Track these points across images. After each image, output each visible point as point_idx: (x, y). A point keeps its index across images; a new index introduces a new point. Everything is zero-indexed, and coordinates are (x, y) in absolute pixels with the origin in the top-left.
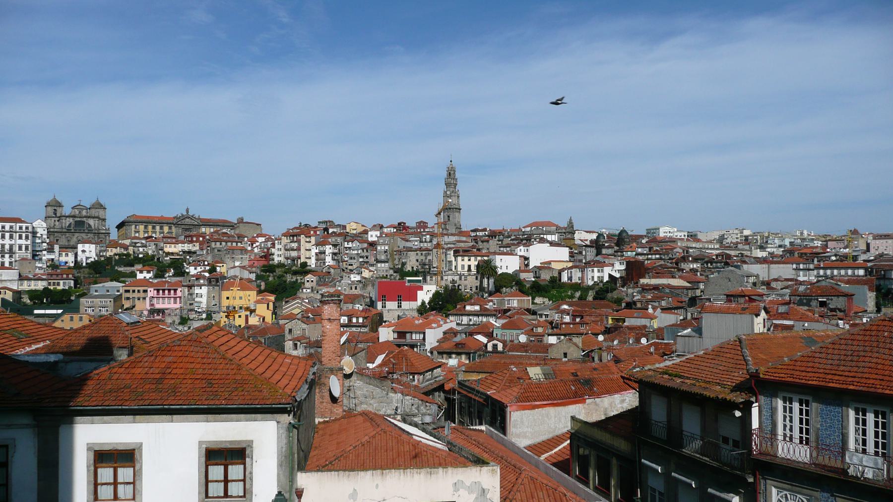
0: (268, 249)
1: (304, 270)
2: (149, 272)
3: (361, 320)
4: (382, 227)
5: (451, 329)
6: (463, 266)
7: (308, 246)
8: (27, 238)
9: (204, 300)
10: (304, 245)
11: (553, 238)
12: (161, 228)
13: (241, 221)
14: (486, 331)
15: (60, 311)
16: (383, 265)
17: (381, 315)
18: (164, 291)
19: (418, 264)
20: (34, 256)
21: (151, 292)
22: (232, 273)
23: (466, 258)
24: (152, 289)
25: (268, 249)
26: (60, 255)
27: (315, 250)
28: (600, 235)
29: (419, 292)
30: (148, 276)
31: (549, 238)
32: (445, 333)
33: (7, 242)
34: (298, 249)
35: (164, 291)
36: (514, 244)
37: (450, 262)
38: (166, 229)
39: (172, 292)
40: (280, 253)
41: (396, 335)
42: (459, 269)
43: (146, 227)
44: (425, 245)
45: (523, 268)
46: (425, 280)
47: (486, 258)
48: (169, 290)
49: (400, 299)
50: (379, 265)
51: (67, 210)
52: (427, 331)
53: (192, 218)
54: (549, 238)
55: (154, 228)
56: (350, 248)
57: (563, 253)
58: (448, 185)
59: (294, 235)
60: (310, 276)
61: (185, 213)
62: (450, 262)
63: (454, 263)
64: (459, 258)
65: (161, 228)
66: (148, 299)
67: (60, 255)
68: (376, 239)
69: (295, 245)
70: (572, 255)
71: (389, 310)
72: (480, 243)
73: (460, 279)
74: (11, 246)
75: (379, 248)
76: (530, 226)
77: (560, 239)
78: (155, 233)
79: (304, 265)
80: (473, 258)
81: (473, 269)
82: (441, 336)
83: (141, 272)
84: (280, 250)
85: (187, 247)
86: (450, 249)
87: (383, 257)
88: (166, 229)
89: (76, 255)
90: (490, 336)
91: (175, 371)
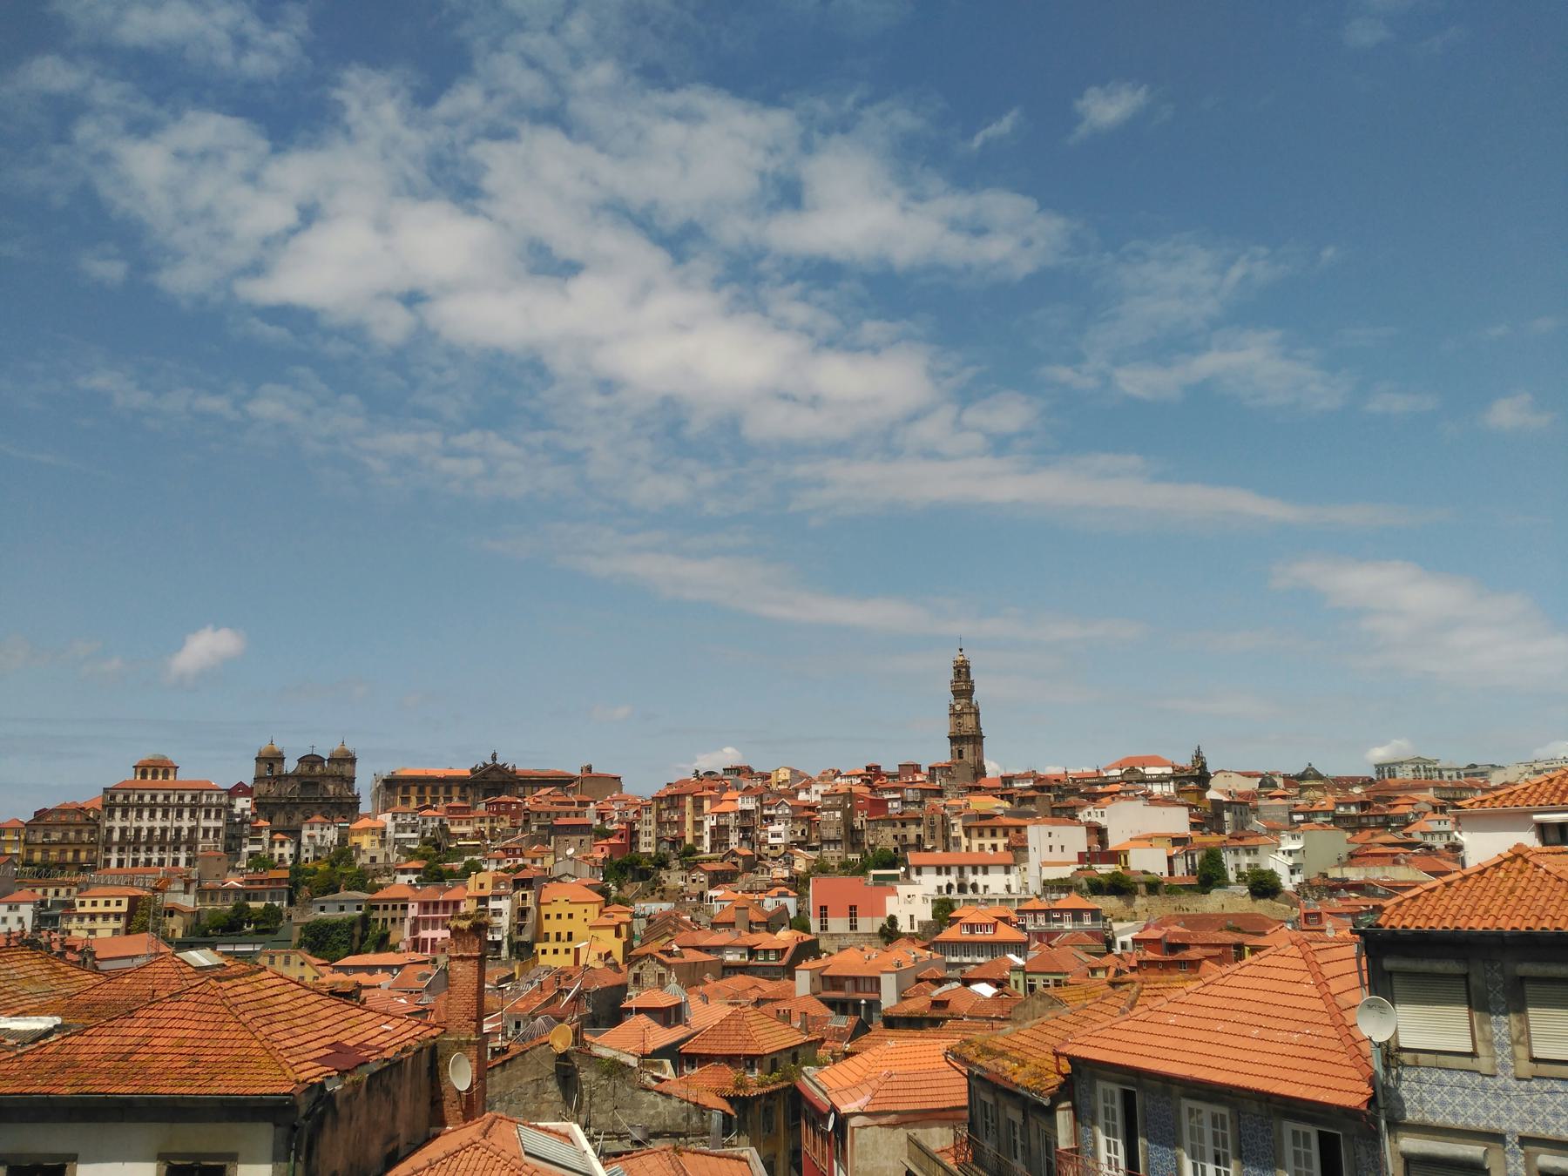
0: (631, 824)
1: (690, 859)
2: (415, 871)
3: (772, 957)
4: (838, 774)
6: (981, 847)
8: (218, 816)
9: (504, 921)
12: (448, 791)
14: (996, 976)
15: (258, 948)
17: (815, 942)
19: (896, 844)
20: (228, 849)
21: (413, 911)
25: (631, 824)
26: (272, 844)
27: (709, 823)
28: (1267, 781)
30: (413, 878)
33: (186, 823)
34: (680, 824)
37: (957, 839)
38: (456, 791)
42: (975, 849)
43: (421, 790)
45: (1097, 847)
46: (907, 874)
51: (290, 766)
52: (883, 978)
54: (1157, 789)
56: (772, 818)
57: (1177, 821)
58: (957, 694)
59: (673, 800)
61: (489, 762)
62: (957, 839)
63: (964, 841)
66: (407, 924)
67: (272, 844)
72: (1016, 801)
74: (192, 830)
77: (1178, 792)
79: (691, 851)
81: (1001, 848)
83: (404, 872)
84: (648, 823)
87: (831, 833)
88: (456, 791)
89: (299, 844)
90: (999, 984)
91: (155, 1042)
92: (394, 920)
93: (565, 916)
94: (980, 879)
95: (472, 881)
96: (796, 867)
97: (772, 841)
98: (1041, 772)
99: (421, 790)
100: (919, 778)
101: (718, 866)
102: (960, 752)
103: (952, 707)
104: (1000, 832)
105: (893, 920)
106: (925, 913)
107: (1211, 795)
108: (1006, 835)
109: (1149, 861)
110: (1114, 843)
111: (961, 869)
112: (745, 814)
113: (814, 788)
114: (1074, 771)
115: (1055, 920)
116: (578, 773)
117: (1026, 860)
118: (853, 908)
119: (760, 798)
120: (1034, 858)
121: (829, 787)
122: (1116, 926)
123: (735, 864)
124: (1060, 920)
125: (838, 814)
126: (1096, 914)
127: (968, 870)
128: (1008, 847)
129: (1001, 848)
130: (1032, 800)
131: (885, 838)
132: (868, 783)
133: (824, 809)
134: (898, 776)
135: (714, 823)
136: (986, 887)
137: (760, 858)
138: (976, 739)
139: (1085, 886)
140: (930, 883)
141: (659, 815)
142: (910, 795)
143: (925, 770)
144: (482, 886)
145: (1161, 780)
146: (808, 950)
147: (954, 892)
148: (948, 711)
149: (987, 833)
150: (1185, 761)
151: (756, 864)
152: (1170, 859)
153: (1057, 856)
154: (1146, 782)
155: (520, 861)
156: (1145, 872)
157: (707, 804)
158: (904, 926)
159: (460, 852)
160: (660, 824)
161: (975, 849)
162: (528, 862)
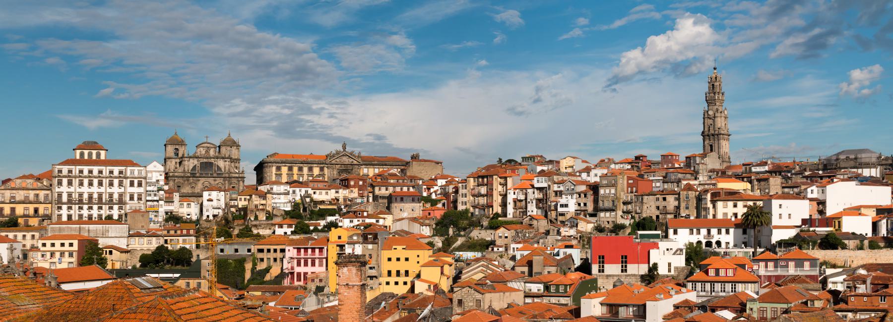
2: (290, 226)
4: (611, 161)
6: (725, 214)
10: (498, 189)
11: (874, 172)
12: (310, 169)
13: (415, 158)
16: (608, 214)
17: (595, 280)
18: (306, 249)
19: (658, 213)
21: (291, 252)
22: (398, 226)
23: (731, 204)
24: (291, 248)
29: (651, 251)
30: (289, 231)
31: (866, 172)
32: (676, 307)
34: (489, 194)
35: (306, 249)
36: (804, 184)
38: (316, 171)
39: (317, 251)
40: (465, 199)
41: (605, 309)
42: (720, 216)
43: (290, 169)
45: (816, 216)
46: (666, 236)
47: (760, 203)
48: (313, 249)
49: (624, 261)
50: (602, 214)
52: (648, 304)
53: (351, 155)
54: (866, 172)
55: (300, 169)
56: (561, 192)
60: (502, 229)
63: (711, 211)
64: (720, 204)
65: (310, 169)
68: (598, 179)
69: (483, 190)
71: (608, 276)
75: (602, 191)
78: (302, 175)
80: (740, 204)
82: (671, 309)
83: (281, 226)
85: (343, 193)
86: (706, 191)
87: (608, 204)
88: (316, 171)
92: (275, 260)
93: (402, 259)
95: (333, 234)
96: (579, 228)
97: (560, 210)
99: (290, 169)
100: (677, 166)
102: (711, 146)
105: (655, 266)
106: (680, 261)
110: (830, 211)
111: (709, 232)
112: (540, 189)
113: (593, 172)
115: (782, 267)
116: (409, 159)
121: (605, 171)
122: (829, 271)
123: (531, 225)
125: (613, 191)
126: (813, 262)
127: (714, 231)
129: (739, 217)
131: (650, 209)
135: (515, 197)
140: (683, 238)
144: (340, 237)
146: (588, 287)
154: (857, 168)
155: (368, 221)
156: (853, 234)
158: (662, 270)
159: (322, 214)
162: (373, 221)
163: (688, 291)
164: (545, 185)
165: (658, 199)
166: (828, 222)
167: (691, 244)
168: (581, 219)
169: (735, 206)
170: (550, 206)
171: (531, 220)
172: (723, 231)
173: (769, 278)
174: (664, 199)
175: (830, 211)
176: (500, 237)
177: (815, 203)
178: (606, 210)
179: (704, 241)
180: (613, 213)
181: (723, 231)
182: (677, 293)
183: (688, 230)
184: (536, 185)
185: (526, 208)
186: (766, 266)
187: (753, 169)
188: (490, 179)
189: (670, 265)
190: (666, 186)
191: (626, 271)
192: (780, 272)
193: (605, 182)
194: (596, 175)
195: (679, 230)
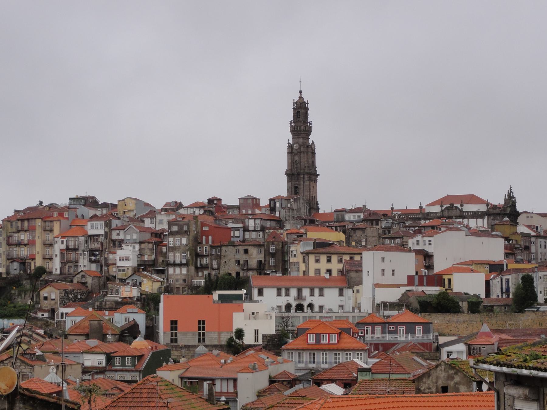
3: (129, 362)
4: (179, 206)
5: (284, 373)
6: (318, 271)
7: (50, 237)
14: (345, 377)
16: (178, 270)
19: (238, 269)
27: (59, 246)
29: (234, 313)
32: (272, 381)
34: (31, 243)
42: (312, 273)
44: (254, 235)
45: (424, 271)
50: (171, 271)
52: (241, 377)
54: (472, 223)
57: (494, 250)
60: (48, 289)
63: (302, 267)
64: (312, 259)
69: (24, 237)
70: (510, 252)
73: (312, 294)
76: (440, 202)
81: (335, 273)
82: (265, 384)
94: (317, 301)
97: (119, 264)
98: (373, 207)
101: (69, 287)
102: (296, 188)
103: (290, 146)
104: (335, 258)
105: (240, 334)
107: (522, 229)
108: (340, 261)
109: (469, 284)
110: (438, 268)
111: (299, 291)
113: (159, 217)
114: (400, 206)
115: (391, 332)
117: (360, 283)
118: (202, 324)
119: (108, 224)
120: (368, 281)
121: (172, 217)
123: (84, 284)
124: (396, 332)
125: (184, 240)
127: (306, 292)
128: (342, 272)
129: (335, 273)
130: (363, 230)
132: (211, 213)
133: (172, 234)
134: (238, 207)
135: (63, 247)
136: (321, 307)
137: (108, 279)
138: (313, 176)
139: (416, 305)
141: (9, 237)
142: (251, 224)
143: (264, 202)
145: (476, 215)
147: (293, 310)
148: (286, 150)
149: (323, 258)
150: (499, 200)
151: (105, 285)
152: (488, 283)
153: (388, 279)
154: (463, 217)
157: (57, 227)
158: (248, 339)
160: (9, 244)
161: (312, 273)
163: (285, 361)
164: (101, 232)
165: (238, 252)
166: (438, 280)
167: (280, 307)
168: (146, 276)
169: (329, 261)
170: (106, 259)
171: (83, 276)
172: (317, 291)
173: (376, 346)
174: (246, 251)
175: (438, 268)
176: (46, 298)
177: (421, 257)
178: (174, 265)
179: (294, 304)
180: (184, 270)
181: (317, 291)
182: (272, 363)
183: (274, 291)
184: (91, 232)
185: (77, 262)
186: (373, 333)
187: (347, 217)
188: (32, 223)
189: (256, 332)
190: (247, 235)
191: (204, 339)
192: (389, 338)
193: (175, 228)
194: (161, 222)
195: (266, 291)
